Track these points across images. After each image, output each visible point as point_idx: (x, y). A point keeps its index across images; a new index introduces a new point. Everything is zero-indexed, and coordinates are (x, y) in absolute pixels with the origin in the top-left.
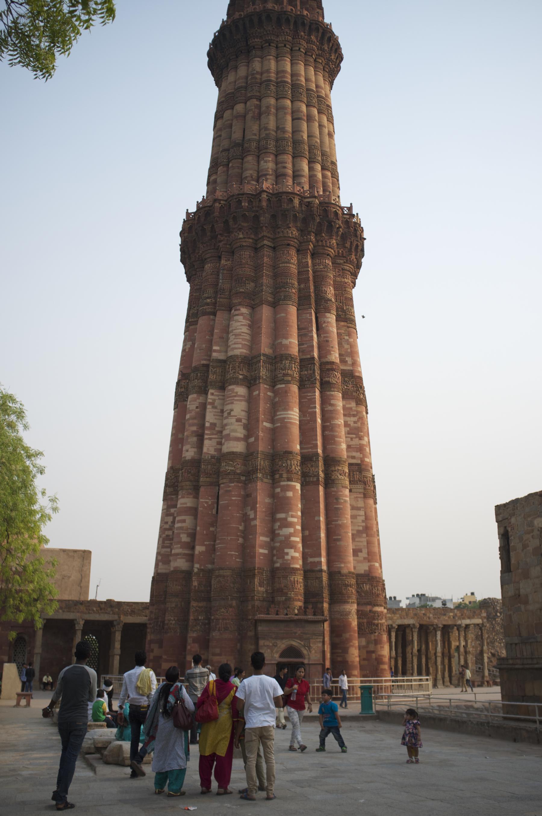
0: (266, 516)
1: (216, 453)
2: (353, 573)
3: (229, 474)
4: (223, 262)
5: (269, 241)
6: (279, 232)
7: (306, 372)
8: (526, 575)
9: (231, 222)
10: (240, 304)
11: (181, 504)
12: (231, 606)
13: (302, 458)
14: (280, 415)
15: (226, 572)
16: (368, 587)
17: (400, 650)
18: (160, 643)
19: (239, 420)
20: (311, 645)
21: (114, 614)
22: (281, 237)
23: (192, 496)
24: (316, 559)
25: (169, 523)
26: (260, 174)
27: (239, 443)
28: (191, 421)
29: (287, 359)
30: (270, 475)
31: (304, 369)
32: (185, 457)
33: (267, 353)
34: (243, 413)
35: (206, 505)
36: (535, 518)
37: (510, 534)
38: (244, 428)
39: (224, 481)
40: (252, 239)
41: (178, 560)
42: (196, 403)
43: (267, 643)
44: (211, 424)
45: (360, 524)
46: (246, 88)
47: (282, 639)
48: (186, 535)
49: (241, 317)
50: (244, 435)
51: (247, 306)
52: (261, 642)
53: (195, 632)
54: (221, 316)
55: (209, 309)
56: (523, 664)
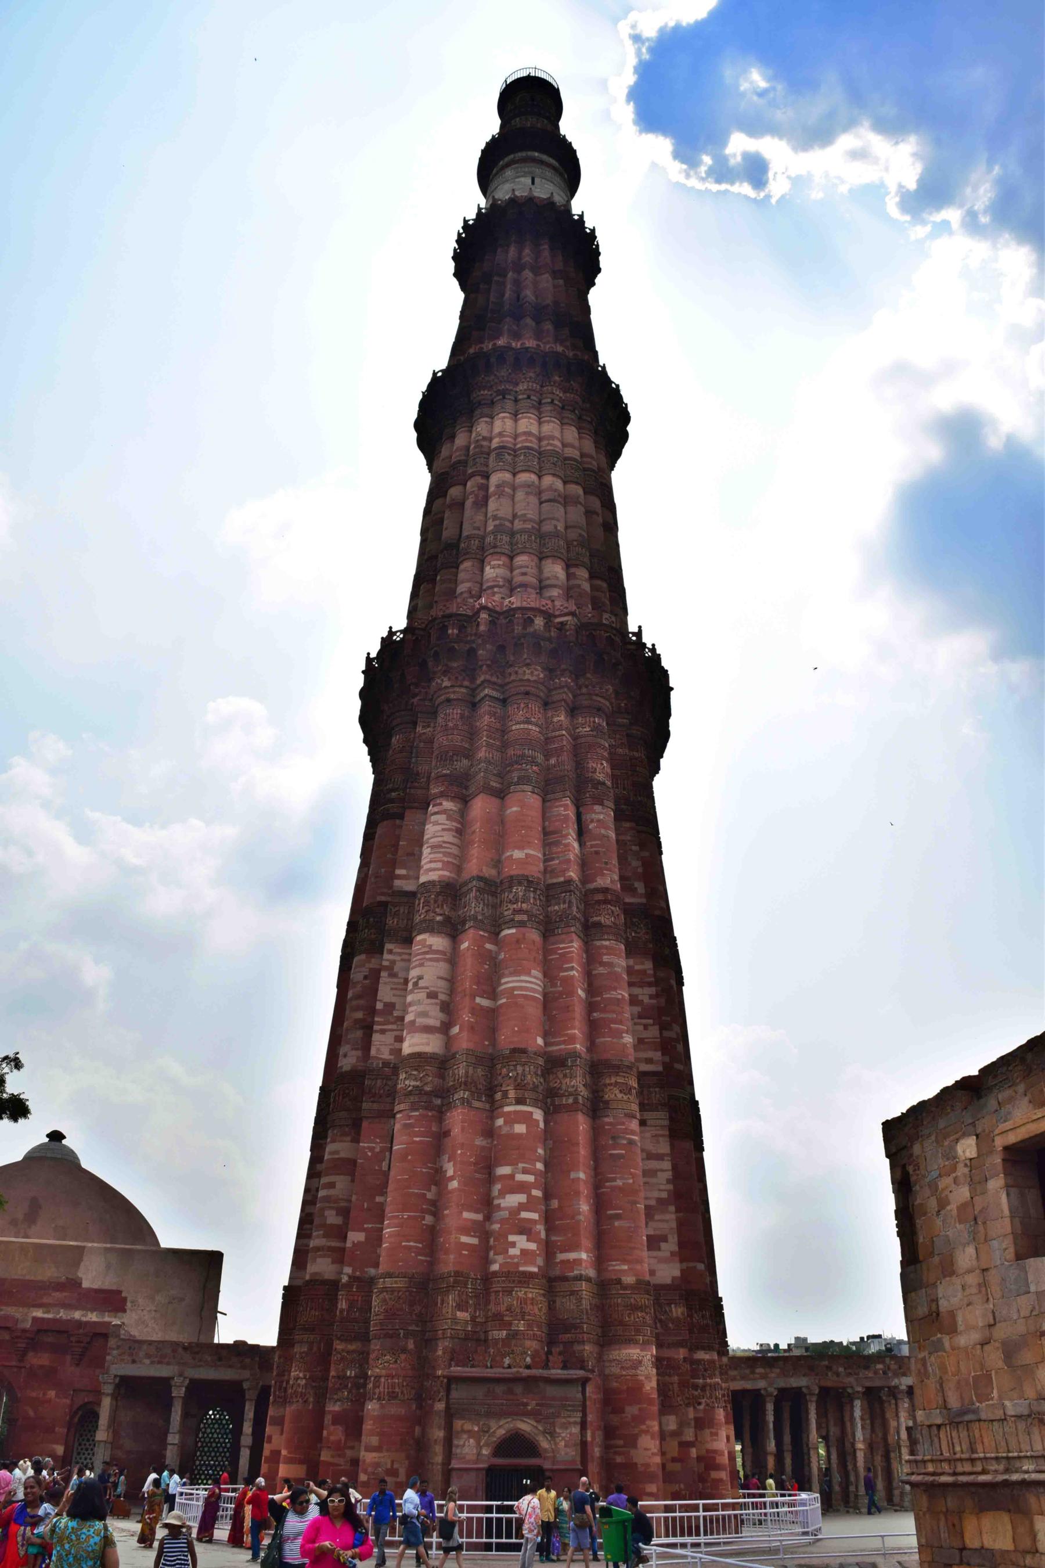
0: (476, 1172)
1: (392, 1057)
2: (648, 1283)
3: (410, 1093)
5: (493, 689)
6: (510, 674)
7: (556, 908)
8: (948, 1269)
10: (442, 795)
11: (330, 1153)
12: (404, 1350)
14: (506, 983)
15: (396, 1282)
16: (680, 1310)
17: (787, 1439)
20: (558, 1430)
21: (244, 1367)
22: (513, 681)
23: (349, 1138)
24: (572, 1256)
26: (484, 587)
27: (431, 1036)
28: (354, 1003)
29: (520, 884)
30: (487, 1095)
31: (553, 902)
32: (341, 1067)
33: (487, 875)
34: (442, 983)
36: (957, 1140)
37: (913, 1179)
38: (442, 1010)
39: (402, 1107)
40: (466, 687)
41: (319, 1260)
42: (363, 969)
43: (468, 1426)
44: (386, 1005)
45: (662, 1187)
48: (334, 1212)
49: (444, 816)
50: (442, 1022)
51: (453, 798)
52: (458, 1424)
53: (339, 1403)
56: (955, 1474)
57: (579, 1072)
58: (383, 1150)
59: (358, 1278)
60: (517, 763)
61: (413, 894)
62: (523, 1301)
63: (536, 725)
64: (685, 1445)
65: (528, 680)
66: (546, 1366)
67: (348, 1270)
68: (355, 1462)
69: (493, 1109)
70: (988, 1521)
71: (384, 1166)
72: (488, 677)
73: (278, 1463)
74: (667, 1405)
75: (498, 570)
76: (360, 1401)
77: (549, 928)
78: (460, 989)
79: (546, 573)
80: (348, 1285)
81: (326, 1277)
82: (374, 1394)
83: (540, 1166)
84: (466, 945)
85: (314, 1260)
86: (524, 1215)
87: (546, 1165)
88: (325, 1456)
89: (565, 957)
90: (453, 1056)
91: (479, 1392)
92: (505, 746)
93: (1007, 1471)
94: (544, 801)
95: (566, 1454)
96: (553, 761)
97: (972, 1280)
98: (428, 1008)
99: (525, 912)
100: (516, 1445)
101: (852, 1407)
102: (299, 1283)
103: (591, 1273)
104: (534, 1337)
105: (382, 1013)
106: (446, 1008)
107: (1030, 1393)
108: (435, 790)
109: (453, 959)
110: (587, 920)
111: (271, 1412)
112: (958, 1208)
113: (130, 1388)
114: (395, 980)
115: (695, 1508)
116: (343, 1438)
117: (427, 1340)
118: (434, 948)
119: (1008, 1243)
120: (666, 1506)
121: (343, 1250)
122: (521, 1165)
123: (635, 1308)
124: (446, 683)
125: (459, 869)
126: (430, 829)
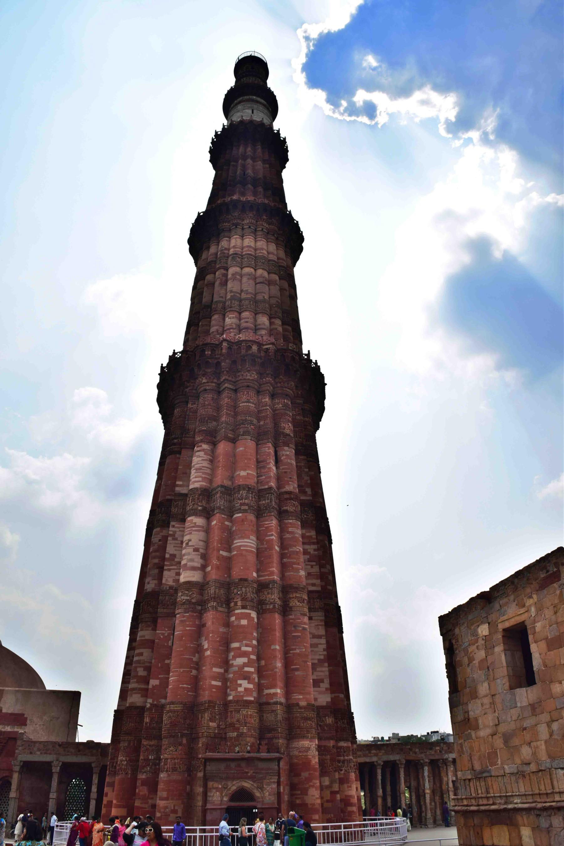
0: (220, 646)
1: (174, 584)
2: (313, 705)
5: (230, 384)
6: (239, 376)
7: (264, 502)
8: (474, 695)
10: (202, 441)
11: (141, 637)
12: (180, 744)
13: (258, 586)
14: (236, 543)
15: (176, 707)
16: (330, 720)
17: (388, 788)
20: (264, 786)
21: (92, 755)
22: (241, 379)
23: (150, 628)
24: (272, 691)
26: (225, 329)
27: (195, 572)
28: (154, 554)
29: (244, 489)
30: (226, 604)
32: (146, 590)
33: (226, 485)
34: (202, 543)
35: (162, 637)
36: (478, 626)
37: (455, 647)
38: (201, 558)
39: (180, 611)
40: (215, 383)
41: (134, 696)
42: (159, 536)
43: (216, 785)
44: (171, 555)
45: (321, 653)
46: (215, 262)
47: (233, 779)
48: (142, 669)
50: (202, 565)
51: (208, 443)
52: (210, 784)
53: (145, 774)
56: (478, 805)
57: (276, 591)
59: (155, 705)
60: (243, 424)
61: (186, 495)
62: (246, 716)
63: (253, 403)
64: (333, 793)
65: (249, 379)
66: (258, 751)
67: (150, 701)
68: (154, 806)
69: (229, 612)
70: (496, 830)
71: (170, 643)
72: (227, 377)
73: (111, 807)
74: (324, 772)
76: (156, 773)
77: (260, 513)
78: (211, 547)
80: (150, 709)
81: (138, 705)
82: (164, 768)
83: (255, 642)
84: (215, 522)
85: (131, 695)
86: (246, 669)
87: (258, 641)
88: (137, 803)
89: (268, 529)
90: (208, 583)
91: (222, 766)
92: (236, 414)
93: (506, 803)
94: (257, 445)
95: (269, 799)
96: (262, 423)
97: (486, 701)
98: (194, 557)
99: (247, 505)
100: (242, 795)
101: (423, 770)
102: (122, 708)
103: (283, 700)
104: (252, 736)
105: (169, 560)
106: (204, 557)
107: (518, 761)
108: (198, 438)
109: (207, 530)
110: (280, 509)
111: (108, 779)
112: (479, 663)
113: (28, 768)
114: (177, 542)
115: (339, 827)
116: (147, 793)
117: (193, 739)
118: (197, 524)
119: (506, 680)
120: (323, 826)
121: (147, 690)
122: (244, 642)
123: (306, 719)
124: (204, 381)
125: (211, 481)
126: (195, 460)
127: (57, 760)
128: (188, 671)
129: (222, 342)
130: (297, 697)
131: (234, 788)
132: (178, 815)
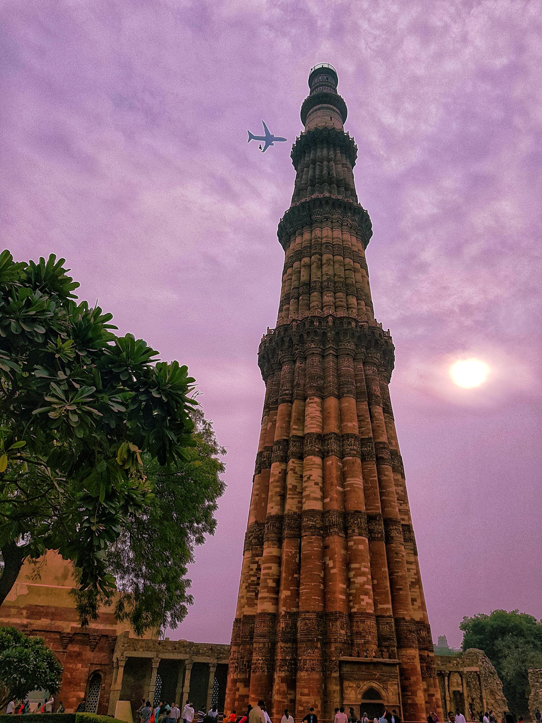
4: (298, 364)
9: (305, 336)
10: (314, 395)
11: (267, 553)
12: (316, 648)
15: (311, 615)
16: (424, 634)
18: (247, 682)
19: (316, 484)
21: (186, 653)
23: (276, 546)
25: (254, 570)
29: (352, 437)
39: (307, 534)
40: (321, 349)
44: (293, 486)
45: (413, 577)
47: (365, 680)
52: (346, 684)
54: (296, 404)
55: (287, 398)
58: (295, 553)
65: (349, 349)
69: (347, 538)
72: (332, 345)
75: (330, 298)
78: (328, 482)
79: (350, 302)
80: (284, 616)
82: (304, 668)
95: (393, 698)
99: (355, 450)
109: (324, 468)
114: (296, 475)
117: (326, 643)
122: (363, 564)
125: (323, 429)
127: (157, 657)
128: (318, 585)
129: (328, 317)
130: (402, 612)
131: (365, 688)
132: (318, 710)
